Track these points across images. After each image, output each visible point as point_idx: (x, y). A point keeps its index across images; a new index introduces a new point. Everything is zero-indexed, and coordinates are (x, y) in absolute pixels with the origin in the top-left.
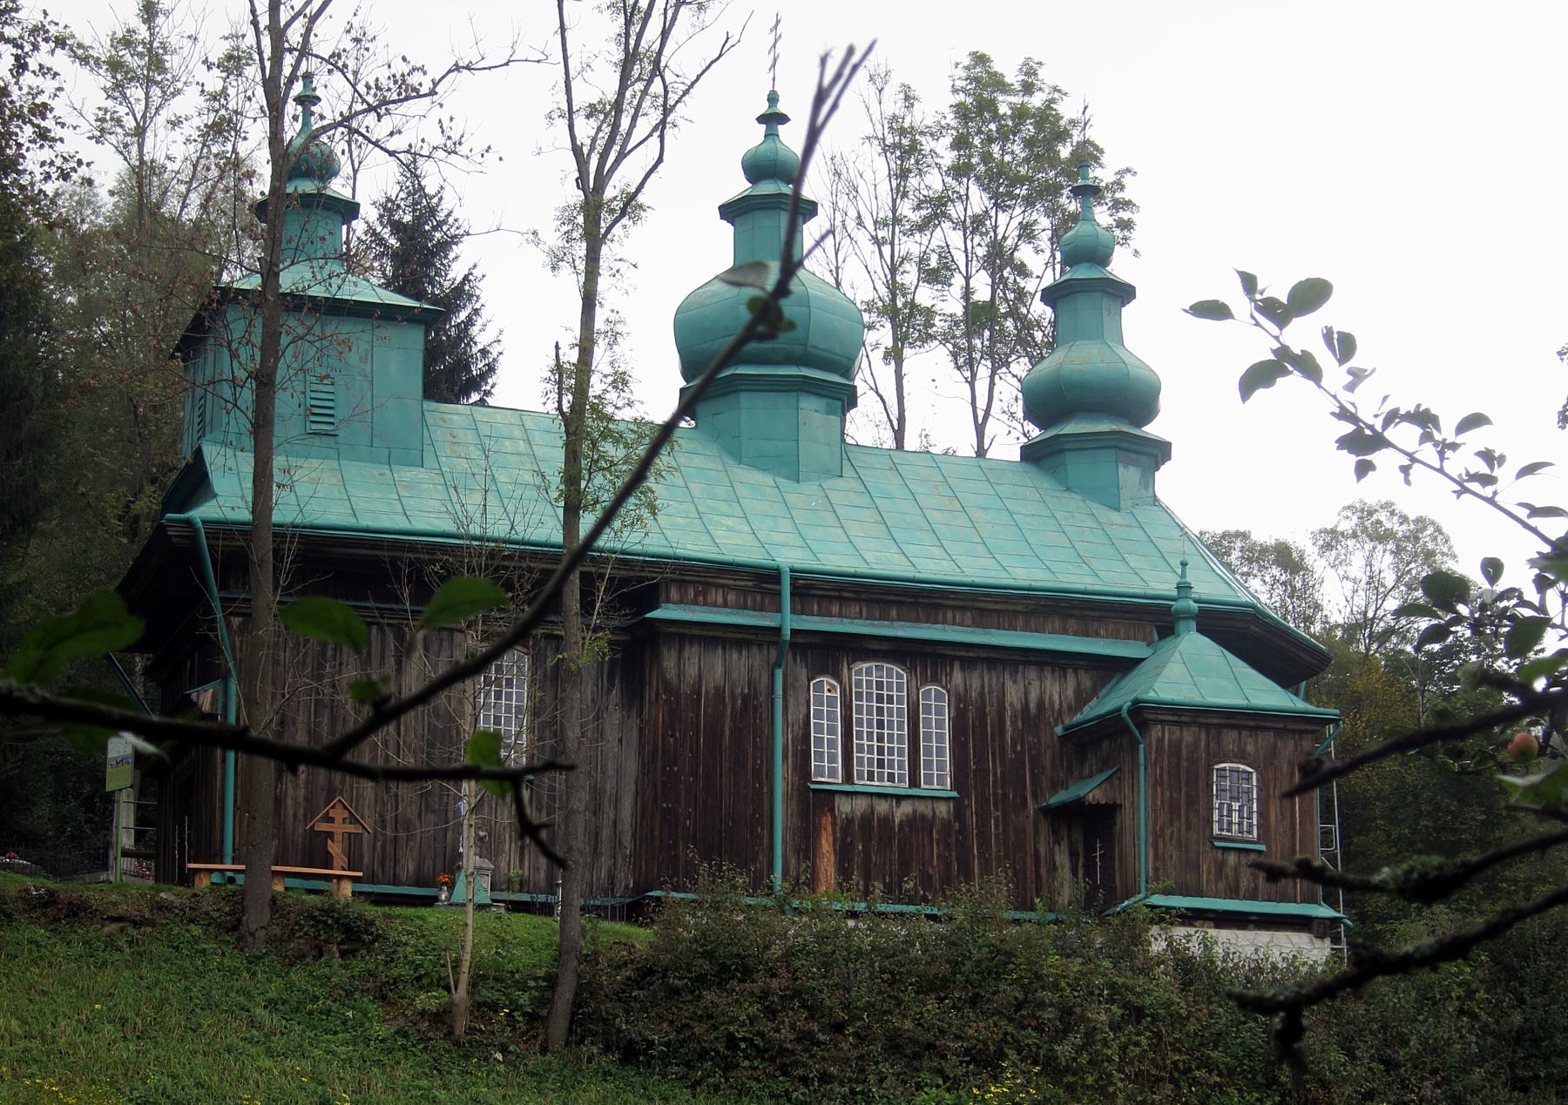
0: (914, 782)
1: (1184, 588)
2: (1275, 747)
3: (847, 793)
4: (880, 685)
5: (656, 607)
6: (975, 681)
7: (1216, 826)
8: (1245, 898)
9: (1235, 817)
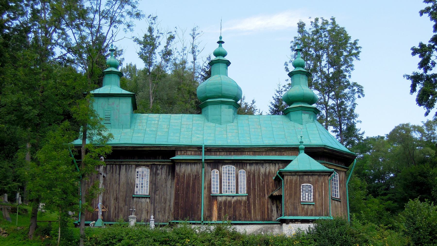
0: (237, 192)
1: (301, 142)
2: (318, 179)
3: (220, 196)
4: (229, 170)
5: (174, 156)
6: (253, 168)
7: (302, 199)
8: (309, 216)
9: (307, 197)
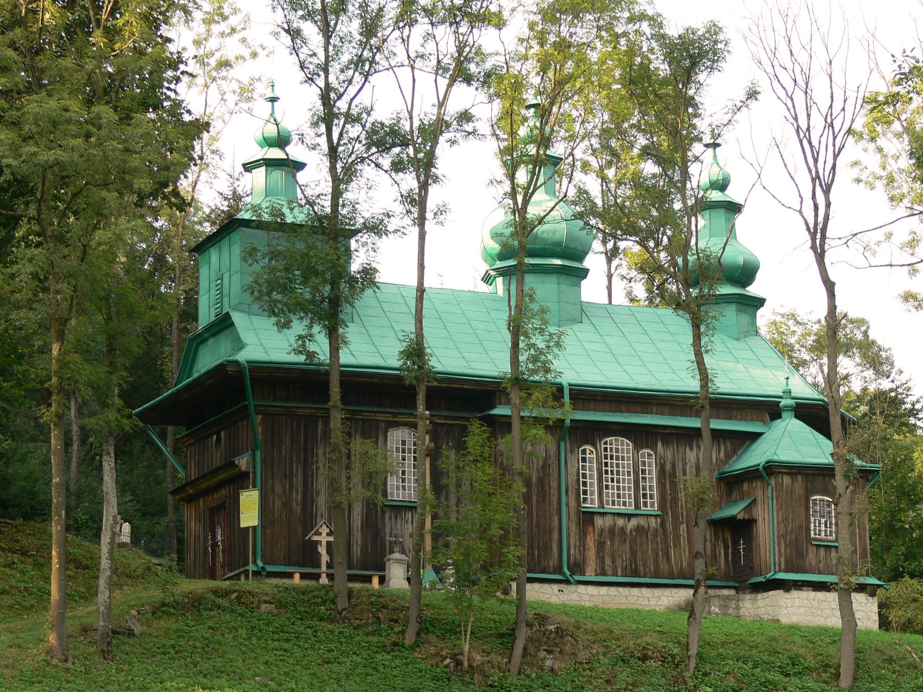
0: (637, 507)
5: (494, 407)
7: (812, 533)
9: (823, 528)
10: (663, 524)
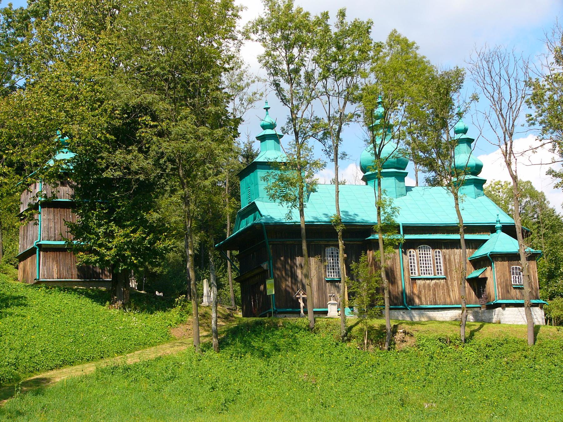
0: (435, 275)
10: (446, 282)
